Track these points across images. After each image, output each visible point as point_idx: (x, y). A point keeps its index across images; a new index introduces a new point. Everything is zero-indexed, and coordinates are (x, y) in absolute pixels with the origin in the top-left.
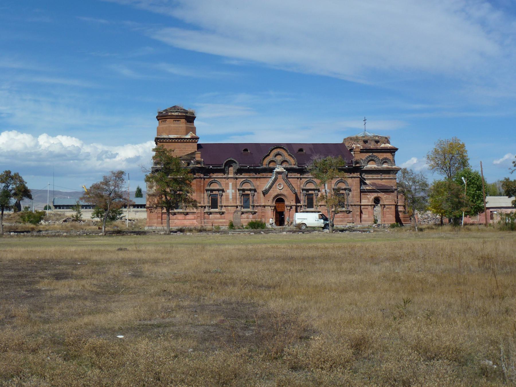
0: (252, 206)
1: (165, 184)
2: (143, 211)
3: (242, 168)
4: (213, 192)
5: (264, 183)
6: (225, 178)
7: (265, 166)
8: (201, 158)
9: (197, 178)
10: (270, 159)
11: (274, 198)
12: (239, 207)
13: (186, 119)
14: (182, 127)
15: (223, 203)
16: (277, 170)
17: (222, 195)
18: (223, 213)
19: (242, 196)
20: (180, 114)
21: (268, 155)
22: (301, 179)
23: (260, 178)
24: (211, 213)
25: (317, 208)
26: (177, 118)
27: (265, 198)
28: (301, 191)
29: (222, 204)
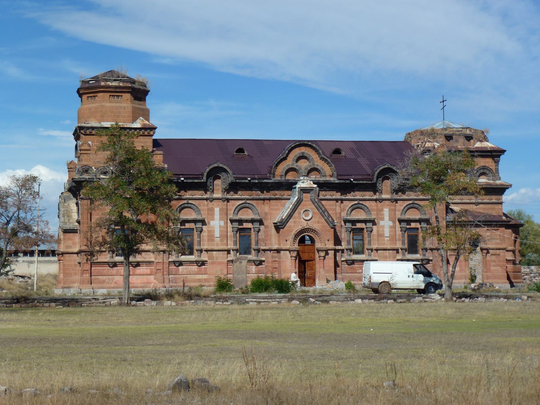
0: (254, 250)
1: (126, 203)
2: (54, 262)
3: (237, 181)
4: (185, 225)
5: (277, 210)
6: (207, 199)
7: (279, 179)
8: (164, 162)
10: (289, 165)
11: (296, 236)
12: (232, 252)
13: (132, 95)
14: (124, 108)
16: (300, 185)
17: (201, 231)
18: (203, 263)
19: (237, 232)
20: (121, 84)
21: (285, 159)
22: (342, 203)
23: (270, 199)
24: (181, 264)
25: (404, 255)
26: (116, 92)
27: (279, 236)
28: (343, 223)
29: (202, 247)
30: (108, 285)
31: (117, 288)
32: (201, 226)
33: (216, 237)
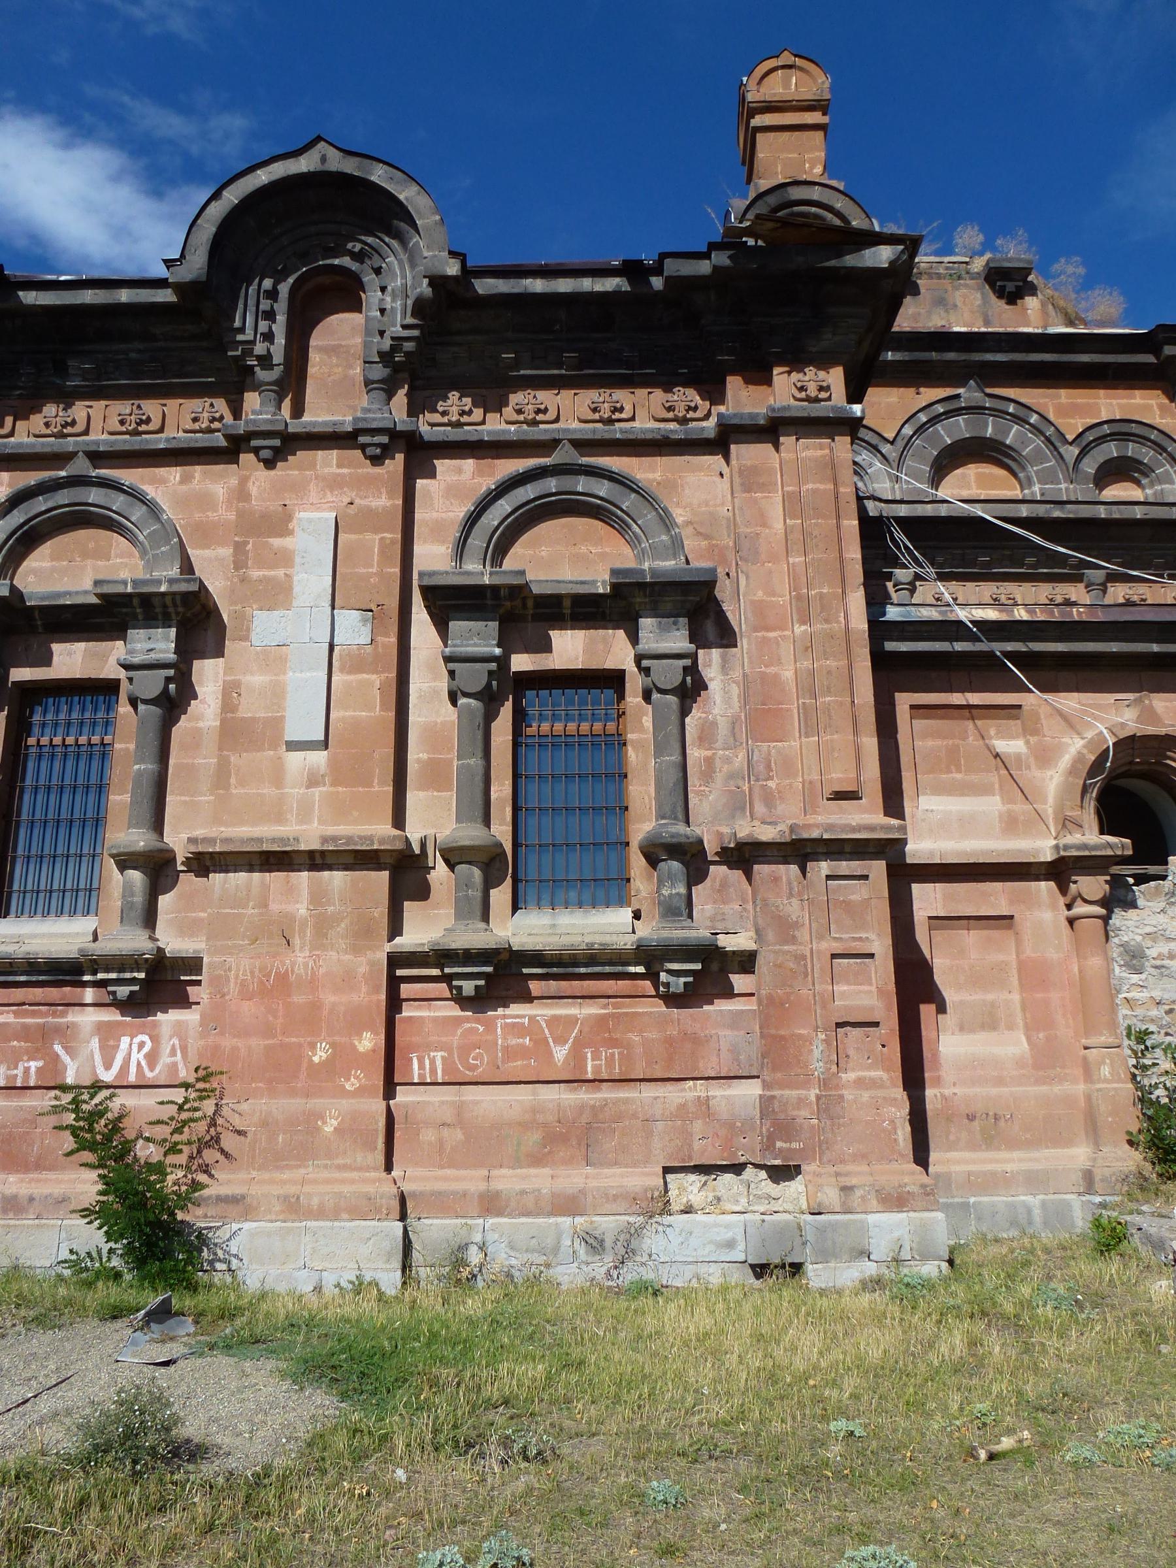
0: (654, 854)
3: (485, 286)
12: (439, 873)
33: (293, 746)
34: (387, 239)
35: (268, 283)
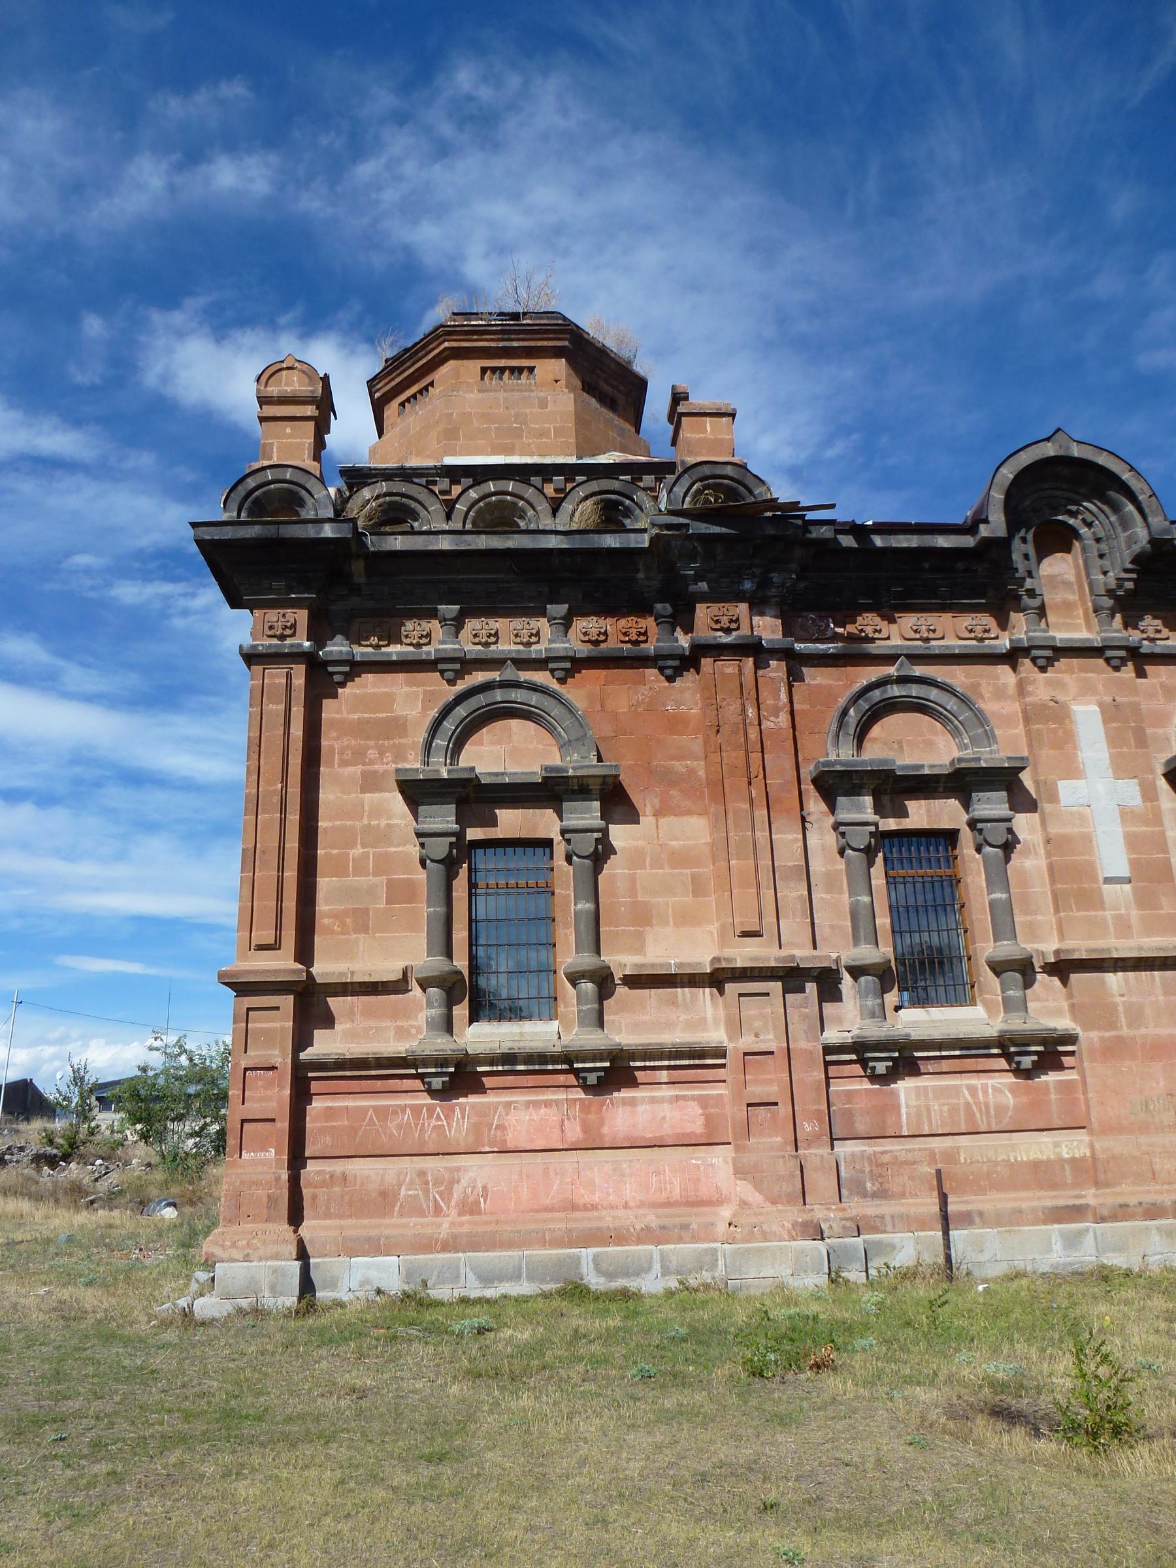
6: (1012, 657)
9: (717, 650)
13: (573, 363)
15: (1033, 932)
30: (415, 1226)
31: (475, 1244)
32: (1003, 810)
33: (1108, 880)
34: (1099, 504)
35: (1022, 533)
